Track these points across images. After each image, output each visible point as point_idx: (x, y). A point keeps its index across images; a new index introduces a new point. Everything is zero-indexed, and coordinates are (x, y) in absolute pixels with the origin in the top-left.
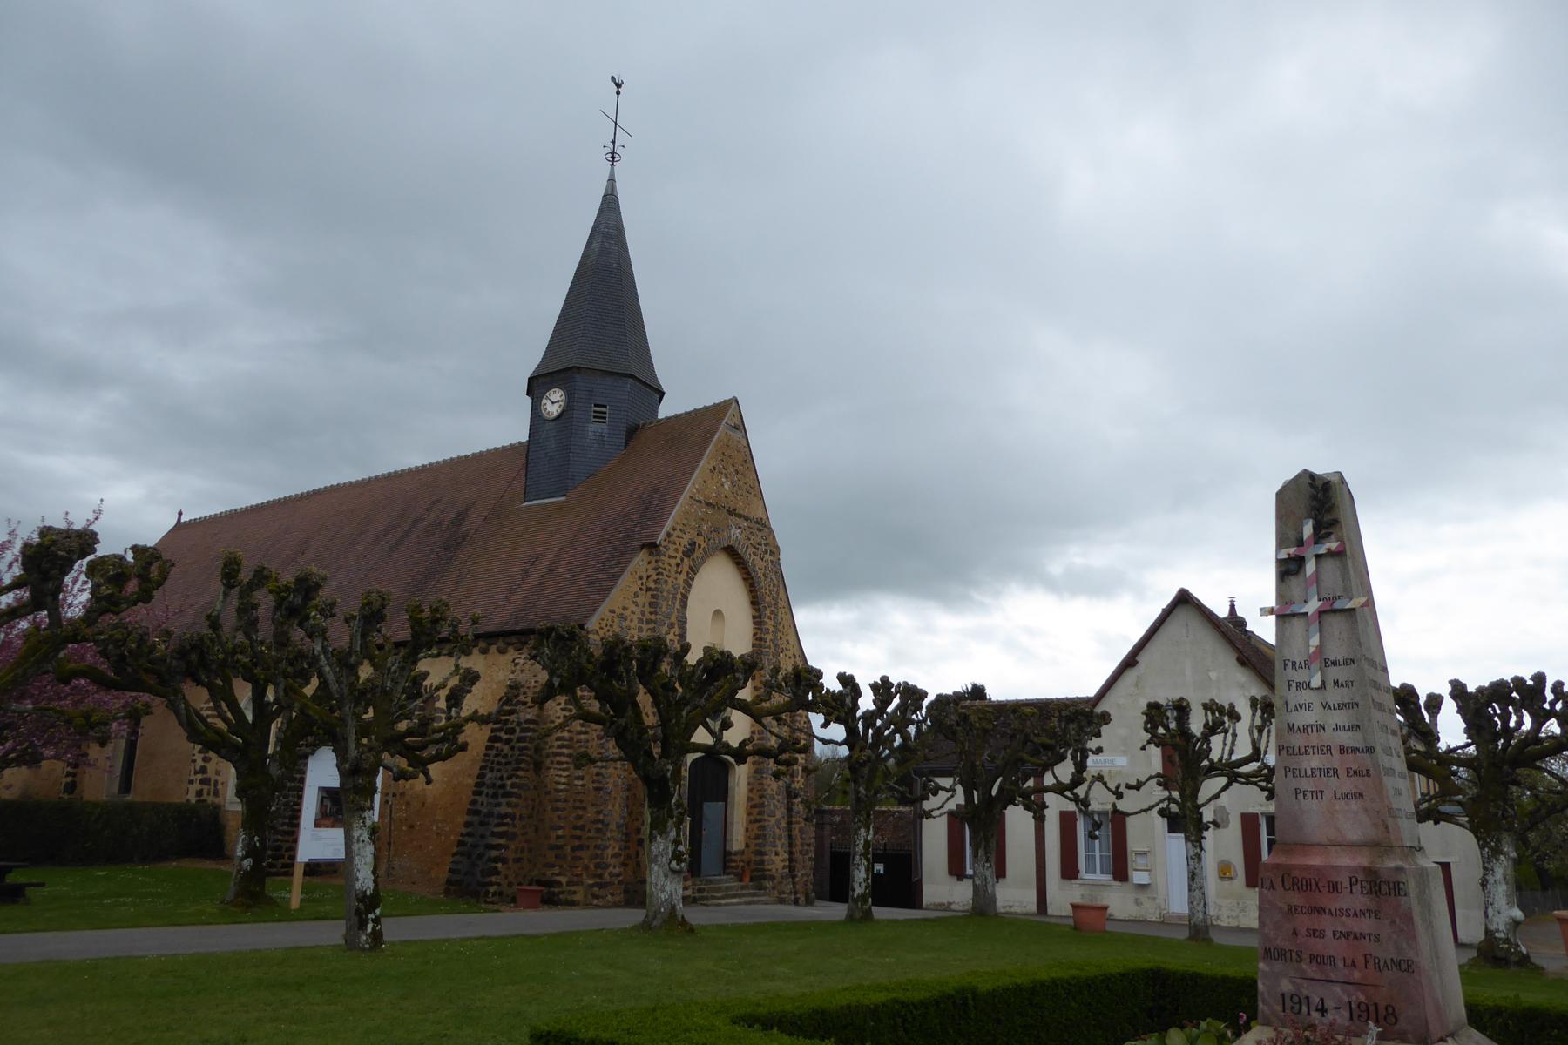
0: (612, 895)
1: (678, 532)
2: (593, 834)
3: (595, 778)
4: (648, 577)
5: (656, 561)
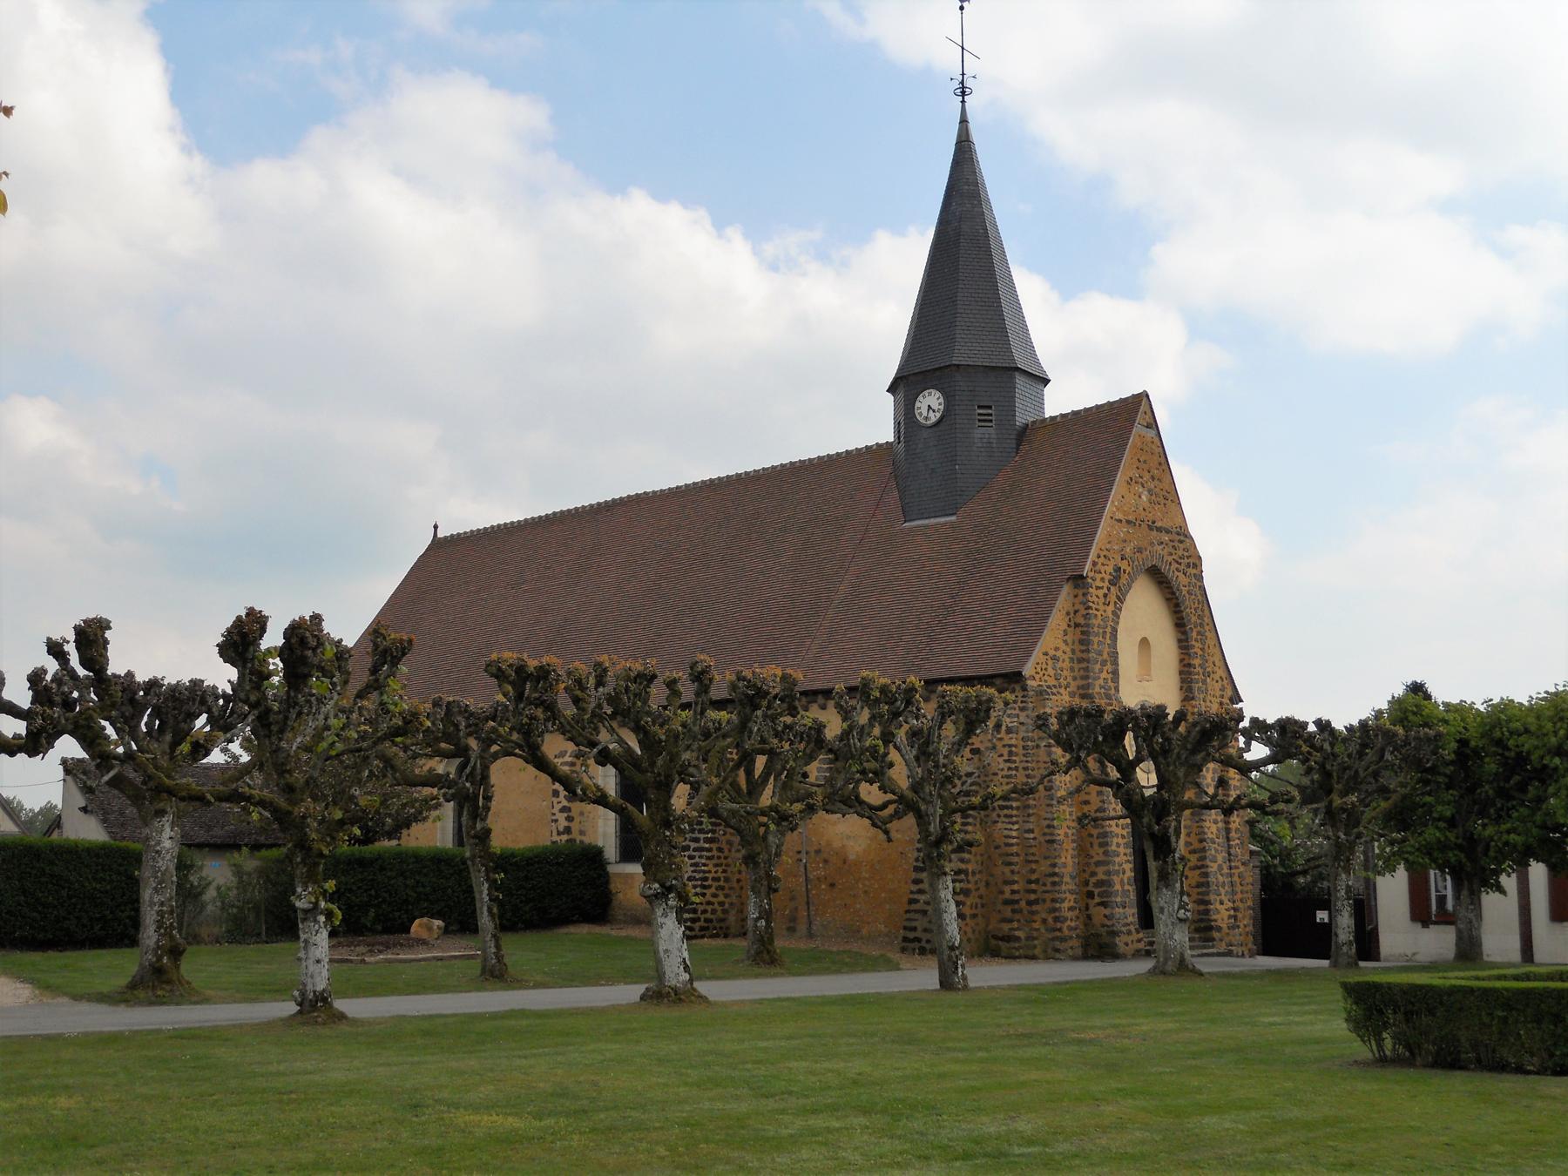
0: (1071, 948)
1: (1102, 560)
2: (1049, 887)
3: (1046, 830)
4: (1076, 612)
5: (1084, 595)
